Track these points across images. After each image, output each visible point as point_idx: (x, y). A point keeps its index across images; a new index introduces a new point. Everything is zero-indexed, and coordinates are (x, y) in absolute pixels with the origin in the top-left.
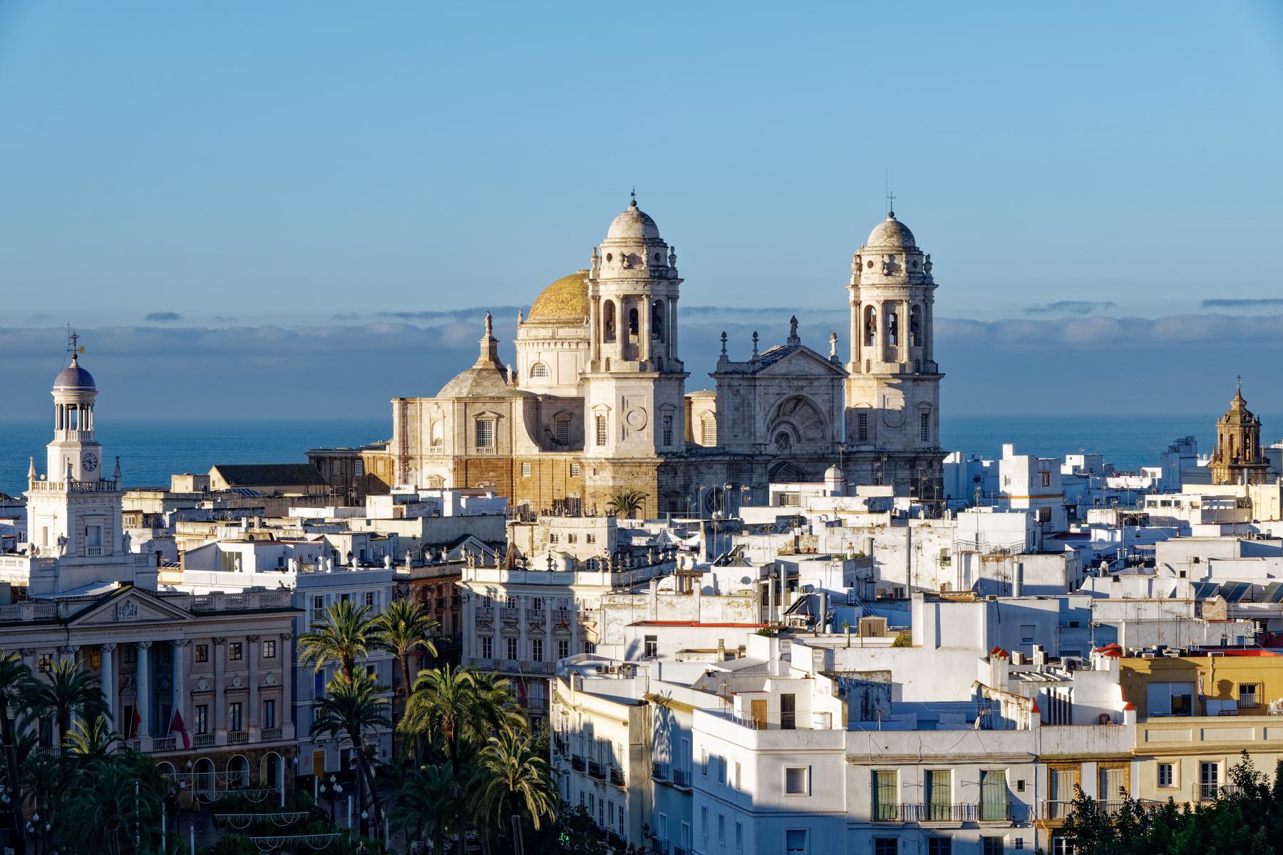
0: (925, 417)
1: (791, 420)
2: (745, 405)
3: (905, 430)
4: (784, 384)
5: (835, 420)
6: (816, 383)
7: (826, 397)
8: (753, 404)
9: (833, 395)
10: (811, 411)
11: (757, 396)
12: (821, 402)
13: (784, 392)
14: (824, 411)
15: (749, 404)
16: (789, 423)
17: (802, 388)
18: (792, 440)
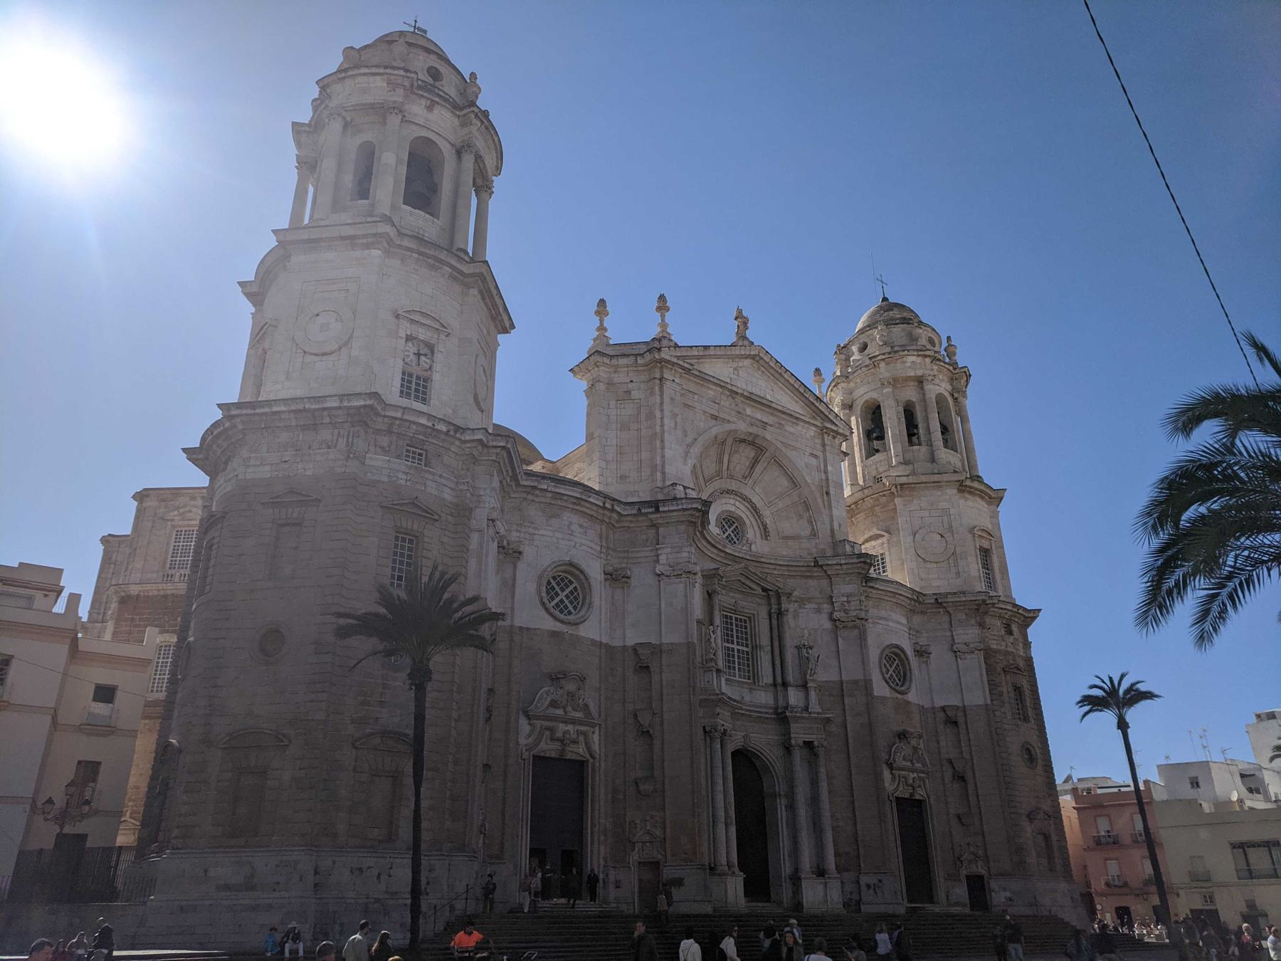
0: (985, 553)
1: (747, 491)
2: (643, 417)
3: (956, 565)
4: (726, 402)
5: (834, 504)
7: (813, 461)
8: (658, 414)
9: (825, 460)
10: (785, 482)
11: (667, 400)
12: (803, 461)
13: (726, 417)
14: (809, 481)
15: (650, 416)
16: (745, 499)
17: (764, 425)
18: (752, 533)
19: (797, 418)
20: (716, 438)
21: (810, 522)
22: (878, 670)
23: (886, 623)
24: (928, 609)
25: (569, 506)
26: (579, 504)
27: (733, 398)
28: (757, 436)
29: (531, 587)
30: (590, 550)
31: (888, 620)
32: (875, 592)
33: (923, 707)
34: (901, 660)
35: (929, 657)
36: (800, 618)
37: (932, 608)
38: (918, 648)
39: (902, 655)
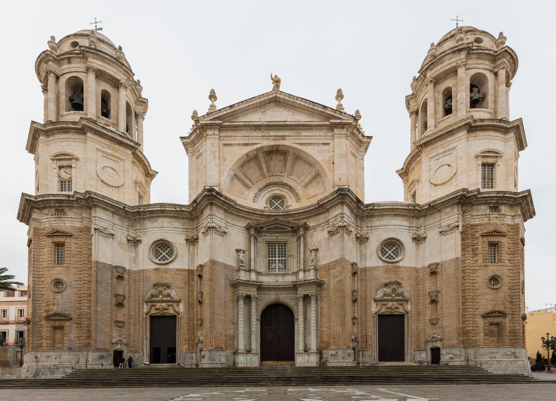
6: (304, 133)
13: (254, 142)
19: (310, 126)
20: (248, 155)
21: (323, 184)
22: (375, 254)
23: (386, 227)
24: (426, 212)
25: (159, 215)
26: (163, 213)
27: (260, 129)
28: (278, 146)
29: (146, 253)
30: (175, 232)
31: (387, 226)
32: (377, 211)
33: (414, 268)
34: (398, 245)
35: (425, 240)
36: (314, 237)
37: (429, 211)
38: (415, 236)
39: (398, 243)
